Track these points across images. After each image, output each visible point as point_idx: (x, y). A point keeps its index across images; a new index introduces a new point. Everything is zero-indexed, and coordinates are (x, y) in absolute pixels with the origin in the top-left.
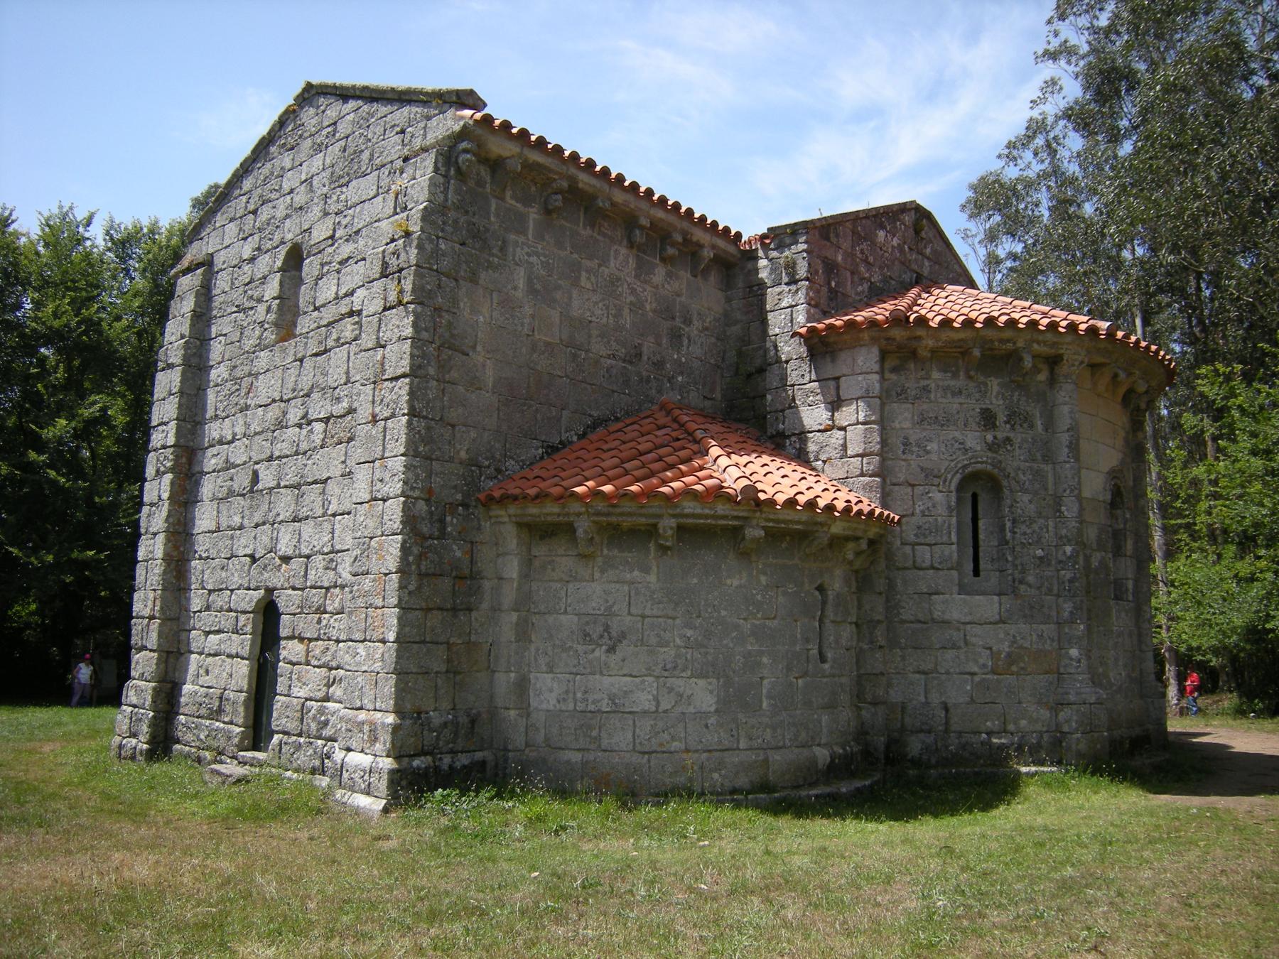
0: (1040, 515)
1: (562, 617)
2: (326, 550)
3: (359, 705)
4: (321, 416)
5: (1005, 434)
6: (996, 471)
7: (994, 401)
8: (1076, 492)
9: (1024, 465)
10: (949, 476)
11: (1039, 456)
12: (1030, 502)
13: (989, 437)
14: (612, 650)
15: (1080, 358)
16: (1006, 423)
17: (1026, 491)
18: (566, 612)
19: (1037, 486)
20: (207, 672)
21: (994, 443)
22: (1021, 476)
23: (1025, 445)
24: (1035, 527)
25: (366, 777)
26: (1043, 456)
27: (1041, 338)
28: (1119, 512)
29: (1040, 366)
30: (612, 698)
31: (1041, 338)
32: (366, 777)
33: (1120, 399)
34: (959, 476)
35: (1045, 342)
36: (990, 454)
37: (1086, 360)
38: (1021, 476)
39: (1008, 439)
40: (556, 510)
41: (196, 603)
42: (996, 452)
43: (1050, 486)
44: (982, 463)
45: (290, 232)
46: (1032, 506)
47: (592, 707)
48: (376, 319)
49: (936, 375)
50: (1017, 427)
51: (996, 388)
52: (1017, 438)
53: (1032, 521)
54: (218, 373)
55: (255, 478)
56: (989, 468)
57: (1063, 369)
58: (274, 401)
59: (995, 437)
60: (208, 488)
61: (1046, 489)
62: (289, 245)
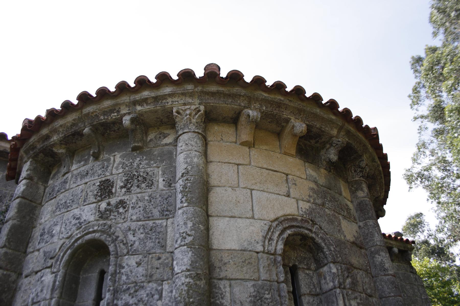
0: (150, 278)
5: (120, 198)
6: (103, 238)
7: (114, 171)
8: (189, 239)
9: (134, 225)
10: (62, 254)
11: (156, 212)
12: (139, 264)
13: (103, 205)
15: (193, 107)
16: (122, 187)
17: (135, 253)
19: (149, 244)
21: (106, 210)
22: (131, 237)
23: (140, 204)
24: (143, 294)
26: (162, 212)
27: (137, 97)
28: (325, 269)
29: (166, 132)
31: (137, 97)
33: (293, 152)
34: (69, 251)
35: (144, 101)
36: (101, 222)
37: (202, 108)
38: (131, 237)
39: (122, 203)
42: (107, 218)
43: (169, 242)
44: (94, 232)
46: (140, 269)
50: (134, 189)
51: (118, 160)
52: (131, 199)
53: (138, 286)
56: (97, 235)
57: (180, 122)
59: (109, 204)
61: (163, 247)
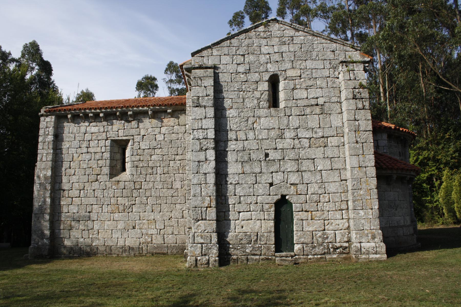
1: (384, 201)
2: (318, 182)
3: (362, 229)
4: (307, 137)
14: (396, 210)
18: (385, 200)
20: (242, 227)
25: (375, 249)
30: (397, 222)
32: (375, 249)
40: (390, 172)
41: (231, 201)
45: (272, 68)
47: (393, 225)
48: (353, 112)
49: (393, 142)
54: (230, 113)
55: (267, 155)
58: (274, 128)
60: (231, 157)
62: (272, 73)
